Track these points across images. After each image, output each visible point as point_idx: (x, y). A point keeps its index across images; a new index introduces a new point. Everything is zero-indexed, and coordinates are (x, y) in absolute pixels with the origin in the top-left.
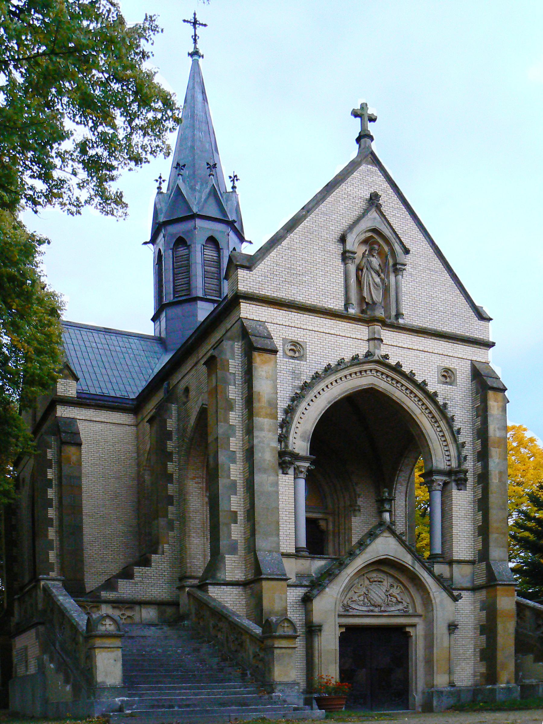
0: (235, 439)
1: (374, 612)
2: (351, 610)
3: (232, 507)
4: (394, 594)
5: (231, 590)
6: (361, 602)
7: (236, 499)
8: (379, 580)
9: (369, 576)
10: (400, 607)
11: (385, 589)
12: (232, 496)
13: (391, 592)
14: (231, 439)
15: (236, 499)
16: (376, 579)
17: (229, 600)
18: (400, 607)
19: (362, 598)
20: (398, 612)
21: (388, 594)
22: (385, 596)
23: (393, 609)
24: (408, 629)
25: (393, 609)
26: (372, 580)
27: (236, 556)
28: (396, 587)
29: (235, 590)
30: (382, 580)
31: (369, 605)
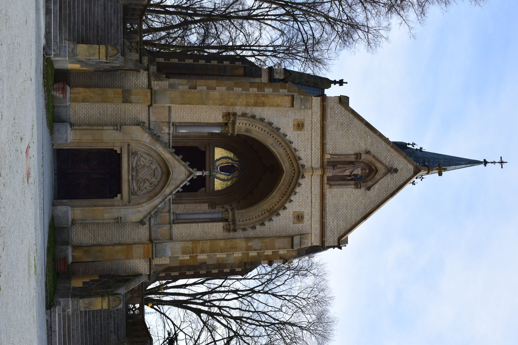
0: (241, 90)
1: (132, 171)
2: (133, 157)
3: (199, 87)
4: (146, 184)
5: (145, 84)
6: (139, 164)
7: (204, 90)
8: (156, 175)
9: (159, 169)
10: (136, 188)
11: (149, 179)
12: (206, 87)
13: (147, 182)
14: (241, 88)
15: (204, 90)
16: (156, 172)
17: (139, 82)
18: (136, 188)
19: (142, 164)
20: (133, 188)
21: (146, 181)
22: (144, 178)
23: (135, 184)
24: (119, 195)
25: (135, 184)
26: (156, 170)
27: (168, 87)
28: (151, 186)
29: (145, 85)
30: (155, 177)
31: (137, 168)
